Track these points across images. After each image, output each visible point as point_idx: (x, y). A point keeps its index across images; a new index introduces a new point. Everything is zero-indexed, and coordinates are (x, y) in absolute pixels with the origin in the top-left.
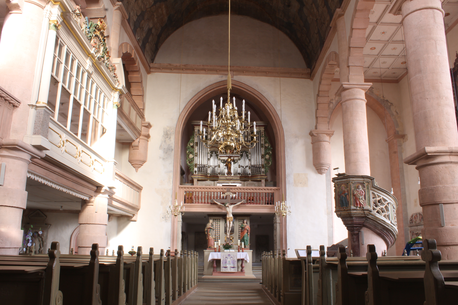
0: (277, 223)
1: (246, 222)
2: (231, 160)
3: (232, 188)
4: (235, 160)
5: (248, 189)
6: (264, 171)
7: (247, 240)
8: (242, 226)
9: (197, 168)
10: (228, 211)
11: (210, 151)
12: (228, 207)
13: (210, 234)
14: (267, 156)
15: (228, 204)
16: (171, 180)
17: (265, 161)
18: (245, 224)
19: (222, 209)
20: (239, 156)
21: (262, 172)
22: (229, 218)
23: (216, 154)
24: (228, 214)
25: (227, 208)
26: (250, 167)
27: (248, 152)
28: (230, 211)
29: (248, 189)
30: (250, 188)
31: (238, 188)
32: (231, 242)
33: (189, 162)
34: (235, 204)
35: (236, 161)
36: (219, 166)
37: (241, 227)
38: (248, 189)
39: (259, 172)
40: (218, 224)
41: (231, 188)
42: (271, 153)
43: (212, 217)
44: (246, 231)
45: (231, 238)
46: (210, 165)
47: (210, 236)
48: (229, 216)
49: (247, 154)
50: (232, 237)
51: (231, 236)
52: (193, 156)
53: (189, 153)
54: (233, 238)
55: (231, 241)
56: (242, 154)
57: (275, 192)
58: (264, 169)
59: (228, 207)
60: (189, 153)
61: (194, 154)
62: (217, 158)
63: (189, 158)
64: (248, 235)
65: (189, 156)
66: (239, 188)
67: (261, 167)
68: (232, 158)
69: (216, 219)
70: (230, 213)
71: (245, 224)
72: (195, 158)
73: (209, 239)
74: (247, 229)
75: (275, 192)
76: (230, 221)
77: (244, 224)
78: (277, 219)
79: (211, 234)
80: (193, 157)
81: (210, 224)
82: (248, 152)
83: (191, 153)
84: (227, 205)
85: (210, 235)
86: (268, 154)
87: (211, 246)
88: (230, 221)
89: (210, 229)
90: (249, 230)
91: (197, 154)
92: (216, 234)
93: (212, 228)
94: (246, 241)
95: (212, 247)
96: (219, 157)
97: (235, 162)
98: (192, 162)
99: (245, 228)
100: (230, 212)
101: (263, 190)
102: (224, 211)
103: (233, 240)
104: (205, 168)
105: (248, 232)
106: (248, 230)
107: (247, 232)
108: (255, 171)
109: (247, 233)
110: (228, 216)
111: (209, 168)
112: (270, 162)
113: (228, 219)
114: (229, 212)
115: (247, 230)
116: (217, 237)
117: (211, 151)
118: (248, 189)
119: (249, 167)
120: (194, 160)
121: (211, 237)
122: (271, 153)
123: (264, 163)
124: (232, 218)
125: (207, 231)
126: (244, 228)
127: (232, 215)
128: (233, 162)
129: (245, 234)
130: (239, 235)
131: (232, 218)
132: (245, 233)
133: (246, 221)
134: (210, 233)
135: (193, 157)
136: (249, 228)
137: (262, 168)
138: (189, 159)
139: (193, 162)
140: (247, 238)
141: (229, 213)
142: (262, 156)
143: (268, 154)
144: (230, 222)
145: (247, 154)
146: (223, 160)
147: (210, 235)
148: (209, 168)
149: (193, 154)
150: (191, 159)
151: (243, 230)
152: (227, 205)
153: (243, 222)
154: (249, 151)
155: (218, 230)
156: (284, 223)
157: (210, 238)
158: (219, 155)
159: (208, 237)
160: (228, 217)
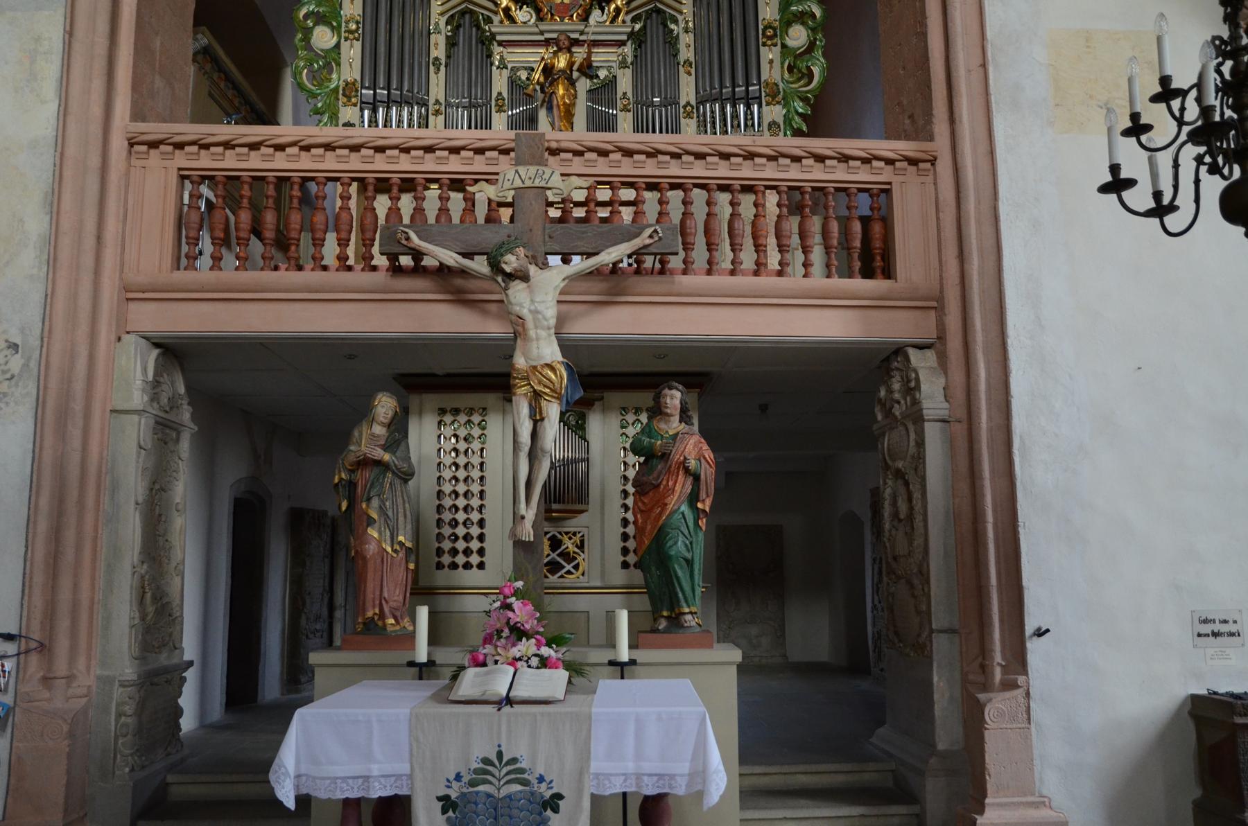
0: (924, 421)
1: (677, 402)
2: (571, 64)
3: (564, 145)
4: (598, 68)
5: (691, 158)
6: (780, 120)
7: (689, 563)
8: (646, 440)
9: (362, 110)
10: (525, 312)
11: (442, 14)
12: (525, 278)
13: (375, 515)
14: (798, 36)
15: (521, 251)
16: (51, 69)
17: (782, 64)
18: (674, 425)
19: (485, 313)
20: (624, 37)
21: (765, 125)
22: (535, 368)
23: (485, 31)
24: (526, 338)
25: (517, 288)
26: (688, 103)
27: (676, 22)
28: (535, 312)
29: (688, 153)
30: (705, 150)
31: (610, 147)
32: (569, 572)
33: (313, 76)
34: (589, 255)
35: (602, 74)
36: (497, 100)
37: (636, 449)
38: (685, 158)
39: (746, 125)
40: (476, 445)
41: (554, 145)
42: (817, 11)
43: (433, 400)
44: (682, 486)
45: (569, 545)
46: (442, 100)
47: (373, 533)
48: (535, 352)
49: (673, 26)
50: (577, 539)
51: (575, 524)
52: (335, 39)
53: (310, 23)
54: (581, 546)
55: (568, 567)
56: (637, 27)
57: (896, 180)
58: (778, 107)
59: (525, 278)
60: (310, 23)
61: (340, 26)
62: (490, 56)
63: (308, 47)
64: (697, 513)
65: (307, 38)
66: (620, 149)
67: (760, 98)
68: (580, 53)
69: (456, 412)
70: (543, 333)
71: (674, 425)
72: (345, 45)
73: (364, 558)
74: (692, 464)
75: (901, 178)
76: (537, 395)
77: (663, 426)
78: (923, 387)
79: (382, 510)
80: (338, 46)
81: (378, 430)
82: (676, 22)
83: (320, 19)
84: (511, 262)
85: (370, 522)
86: (803, 24)
87: (382, 616)
88: (537, 395)
89: (376, 470)
90: (708, 473)
91: (357, 23)
92: (461, 516)
93: (387, 457)
94: (680, 573)
95: (392, 621)
96: (497, 49)
97: (597, 76)
98: (331, 72)
99: (676, 457)
100: (535, 320)
101: (804, 161)
102: (494, 328)
103: (579, 559)
104: (411, 114)
105: (703, 495)
106: (696, 478)
107: (688, 488)
108: (725, 125)
109: (693, 498)
110: (526, 356)
111: (437, 113)
112: (816, 70)
113: (527, 378)
114: (530, 324)
115: (687, 471)
116: (467, 537)
117: (452, 16)
118: (685, 158)
119: (685, 107)
120: (339, 64)
121: (379, 542)
122: (817, 11)
123: (776, 75)
124: (553, 369)
125: (352, 485)
126: (665, 456)
127: (561, 346)
128: (583, 79)
129: (673, 512)
130: (625, 522)
131: (553, 369)
132: (672, 502)
133: (678, 394)
134: (375, 502)
135: (338, 46)
136: (709, 454)
137: (768, 104)
138: (312, 54)
139: (334, 76)
140: (690, 548)
141: (532, 333)
142: (765, 28)
143: (802, 18)
144: (544, 403)
145: (673, 26)
146: (526, 68)
147: (370, 522)
148: (441, 118)
149: (333, 29)
150: (324, 58)
151: (651, 478)
152: (510, 258)
153: (657, 411)
154: (681, 13)
155: (475, 488)
156: (990, 418)
157: (371, 548)
158: (498, 38)
159: (363, 538)
160: (520, 362)
